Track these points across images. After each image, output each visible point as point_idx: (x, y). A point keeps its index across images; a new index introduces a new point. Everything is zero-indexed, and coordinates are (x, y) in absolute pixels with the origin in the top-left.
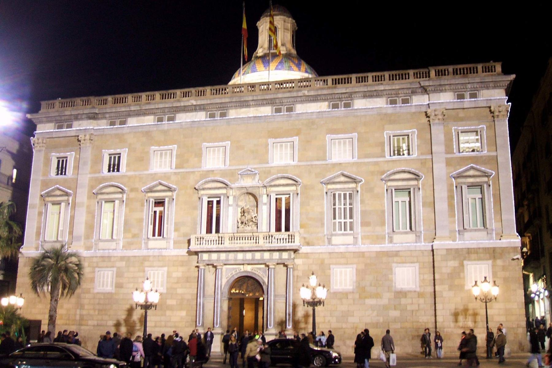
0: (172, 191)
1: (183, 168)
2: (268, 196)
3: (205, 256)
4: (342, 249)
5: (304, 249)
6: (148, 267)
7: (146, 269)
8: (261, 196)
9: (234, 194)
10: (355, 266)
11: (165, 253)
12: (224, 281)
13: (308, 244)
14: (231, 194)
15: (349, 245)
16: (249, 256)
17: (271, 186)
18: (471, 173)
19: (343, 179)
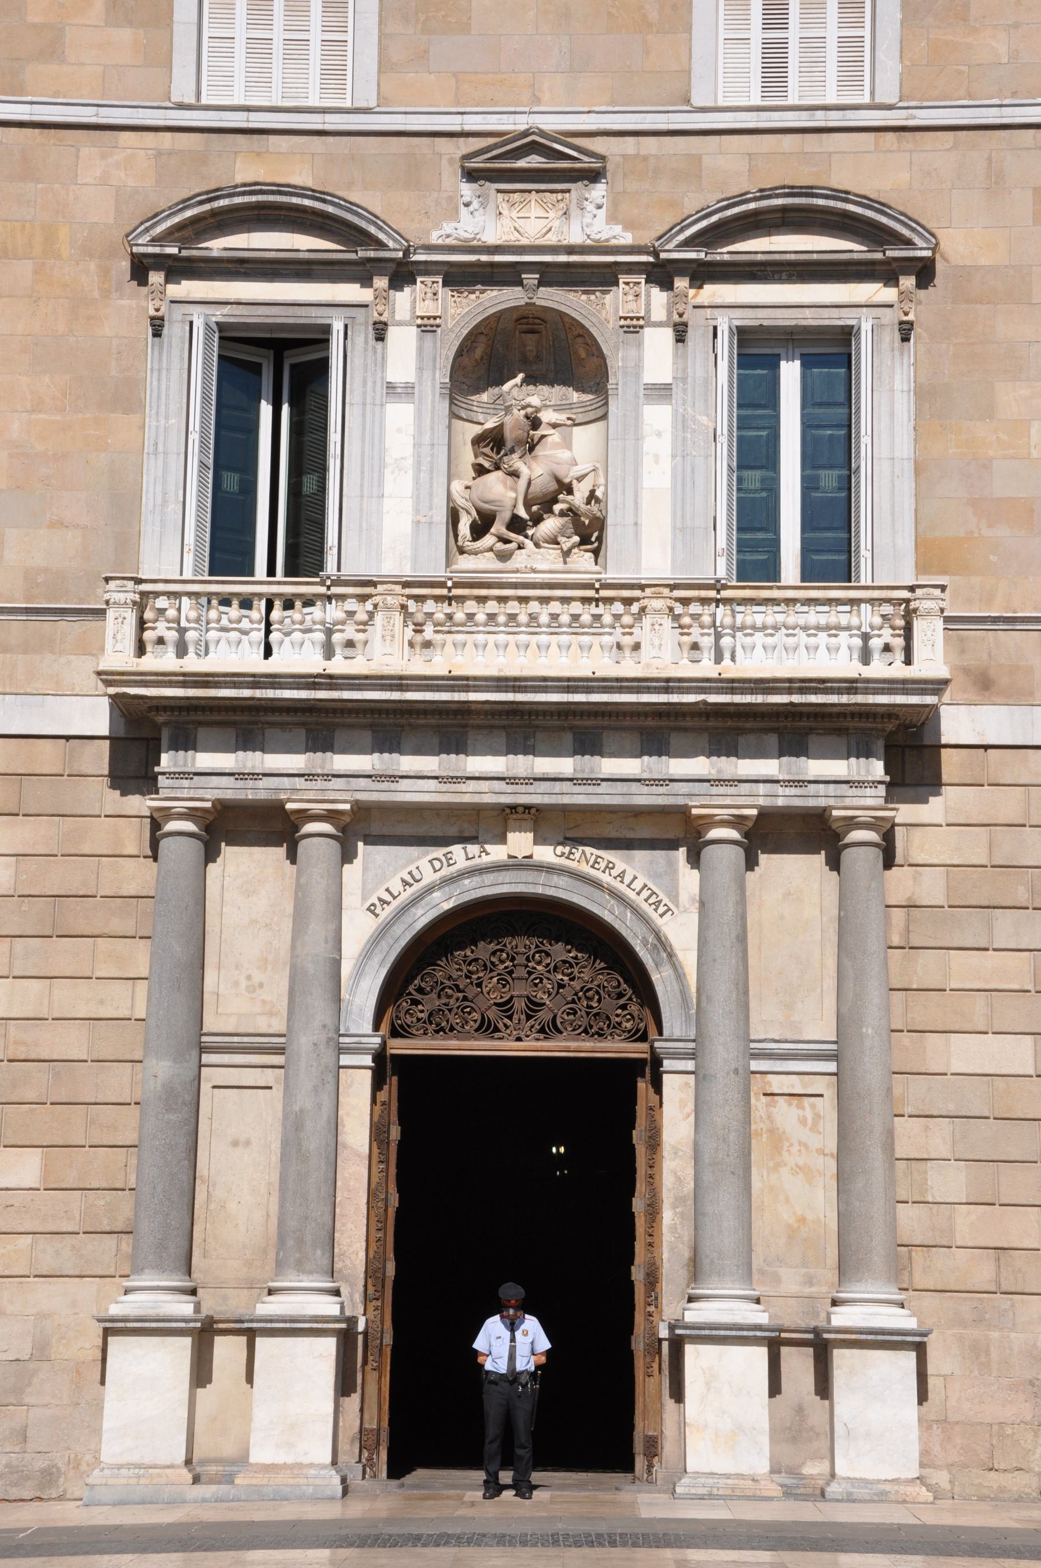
2: (681, 333)
5: (958, 724)
8: (633, 326)
12: (357, 928)
13: (985, 685)
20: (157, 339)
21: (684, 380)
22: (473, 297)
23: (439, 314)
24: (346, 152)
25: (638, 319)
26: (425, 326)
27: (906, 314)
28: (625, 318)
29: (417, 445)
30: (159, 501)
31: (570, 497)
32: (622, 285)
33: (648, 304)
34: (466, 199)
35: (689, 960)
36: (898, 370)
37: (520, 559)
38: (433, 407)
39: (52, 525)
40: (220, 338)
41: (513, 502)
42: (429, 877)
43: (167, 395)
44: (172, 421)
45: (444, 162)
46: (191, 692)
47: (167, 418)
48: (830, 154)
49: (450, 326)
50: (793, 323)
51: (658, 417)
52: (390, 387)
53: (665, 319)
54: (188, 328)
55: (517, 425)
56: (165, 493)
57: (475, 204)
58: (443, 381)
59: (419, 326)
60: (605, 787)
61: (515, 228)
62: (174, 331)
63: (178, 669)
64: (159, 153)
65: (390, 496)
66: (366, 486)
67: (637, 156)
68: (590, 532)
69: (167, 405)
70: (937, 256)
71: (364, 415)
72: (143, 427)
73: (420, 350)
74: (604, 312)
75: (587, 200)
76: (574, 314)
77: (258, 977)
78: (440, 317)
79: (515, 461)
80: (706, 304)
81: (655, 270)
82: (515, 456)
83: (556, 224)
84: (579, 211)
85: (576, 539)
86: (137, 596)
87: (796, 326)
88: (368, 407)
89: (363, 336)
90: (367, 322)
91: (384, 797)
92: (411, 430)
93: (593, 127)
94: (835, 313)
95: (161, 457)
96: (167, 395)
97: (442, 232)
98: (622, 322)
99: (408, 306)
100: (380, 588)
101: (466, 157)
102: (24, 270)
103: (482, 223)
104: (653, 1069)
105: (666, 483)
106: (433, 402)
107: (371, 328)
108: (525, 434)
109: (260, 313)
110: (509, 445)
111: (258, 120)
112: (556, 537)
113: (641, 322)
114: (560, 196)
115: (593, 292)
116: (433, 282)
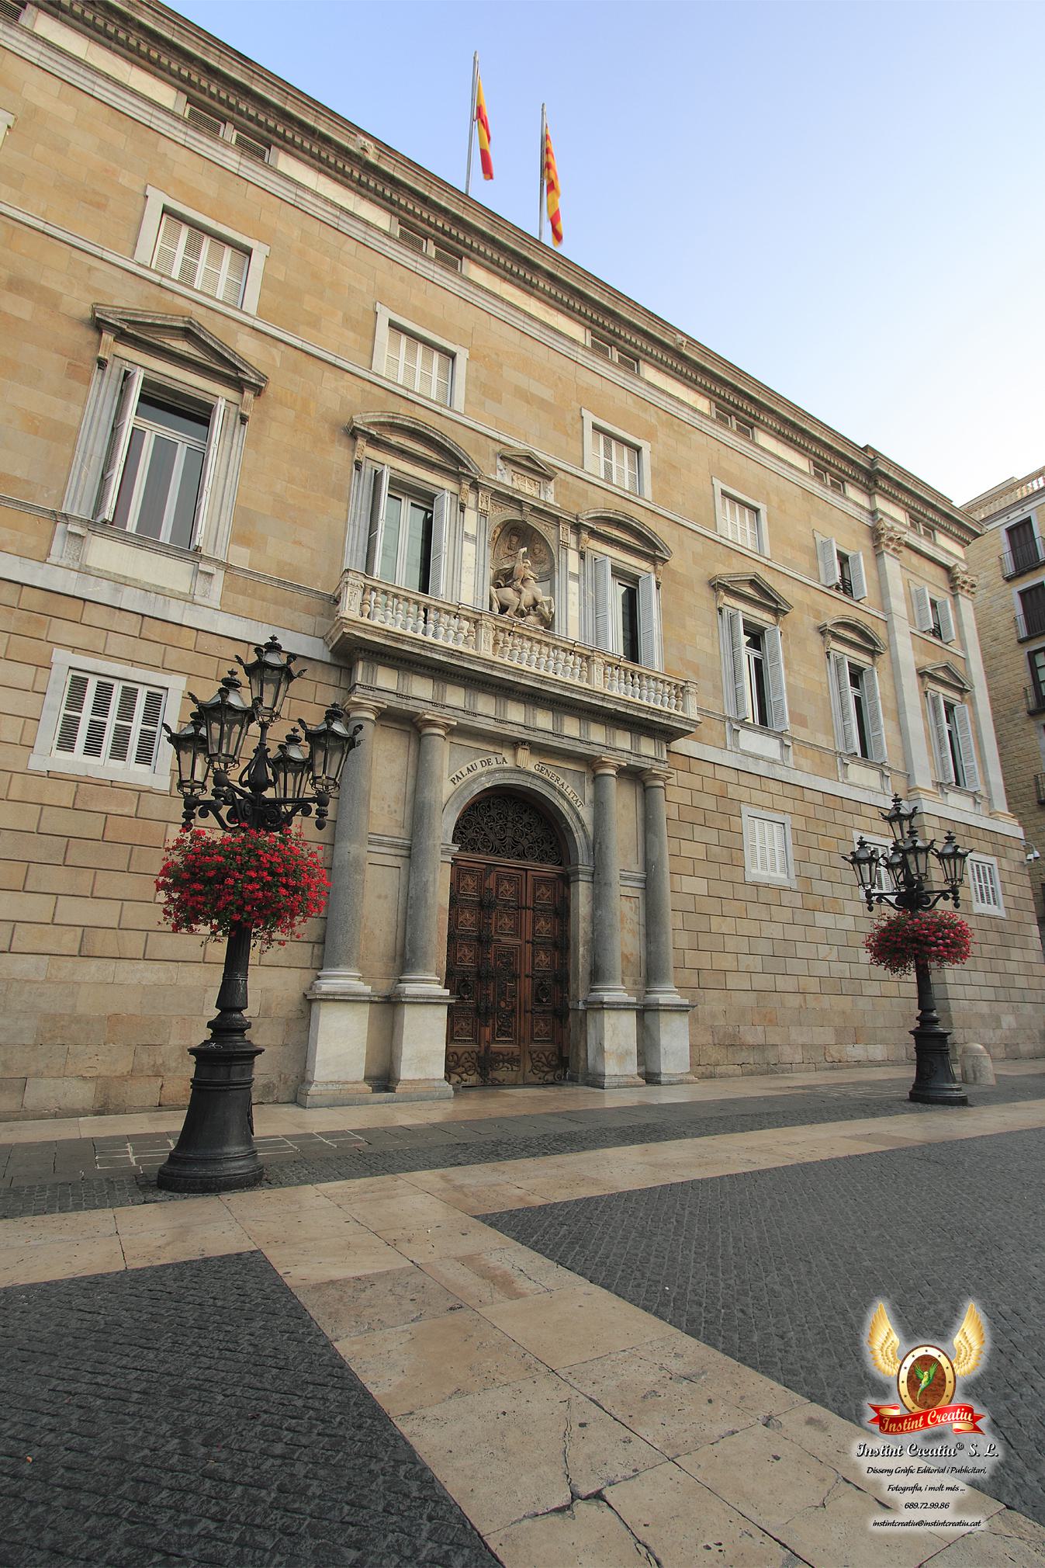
0: (239, 385)
1: (294, 331)
2: (582, 556)
3: (386, 679)
4: (761, 769)
6: (74, 649)
7: (63, 658)
8: (566, 546)
10: (787, 819)
11: (175, 612)
12: (447, 789)
15: (774, 762)
16: (544, 720)
17: (593, 534)
18: (941, 674)
19: (748, 590)
35: (590, 828)
39: (295, 542)
42: (480, 769)
46: (388, 643)
51: (573, 586)
52: (467, 534)
60: (565, 740)
64: (363, 390)
68: (548, 623)
73: (479, 524)
77: (394, 807)
91: (470, 723)
102: (291, 414)
104: (566, 880)
111: (411, 396)
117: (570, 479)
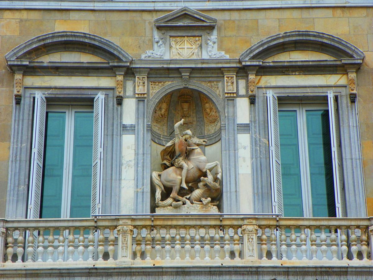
2: (252, 100)
8: (232, 98)
9: (140, 89)
14: (129, 91)
20: (18, 106)
21: (255, 122)
22: (160, 84)
23: (146, 92)
24: (104, 19)
25: (233, 93)
26: (140, 98)
27: (353, 90)
28: (228, 93)
29: (137, 154)
30: (17, 182)
31: (206, 178)
32: (226, 79)
33: (237, 87)
34: (157, 40)
36: (351, 117)
37: (184, 210)
38: (144, 136)
40: (47, 105)
41: (180, 181)
43: (22, 133)
44: (24, 145)
45: (147, 24)
47: (21, 143)
48: (314, 18)
49: (150, 98)
50: (302, 95)
51: (244, 139)
52: (124, 127)
53: (245, 94)
54: (32, 100)
55: (181, 144)
56: (19, 180)
57: (161, 43)
58: (148, 124)
59: (137, 98)
61: (178, 53)
62: (26, 102)
63: (23, 268)
65: (124, 180)
66: (113, 174)
67: (230, 20)
69: (22, 137)
70: (364, 64)
71: (113, 140)
72: (9, 148)
73: (138, 109)
74: (218, 91)
75: (209, 40)
76: (205, 92)
78: (146, 94)
79: (181, 161)
80: (263, 87)
81: (240, 71)
82: (181, 159)
83: (196, 51)
84: (206, 45)
85: (209, 199)
86: (5, 230)
87: (304, 96)
88: (114, 136)
89: (112, 103)
90: (113, 97)
92: (134, 147)
93: (211, 8)
94: (320, 90)
95: (18, 162)
96: (22, 133)
97: (147, 55)
98: (226, 95)
99: (132, 89)
100: (121, 222)
101: (157, 21)
103: (163, 51)
105: (249, 171)
106: (144, 134)
107: (115, 99)
108: (185, 149)
109: (65, 93)
110: (177, 153)
112: (200, 198)
113: (235, 95)
114: (197, 38)
115: (213, 81)
116: (143, 78)
117: (235, 16)
